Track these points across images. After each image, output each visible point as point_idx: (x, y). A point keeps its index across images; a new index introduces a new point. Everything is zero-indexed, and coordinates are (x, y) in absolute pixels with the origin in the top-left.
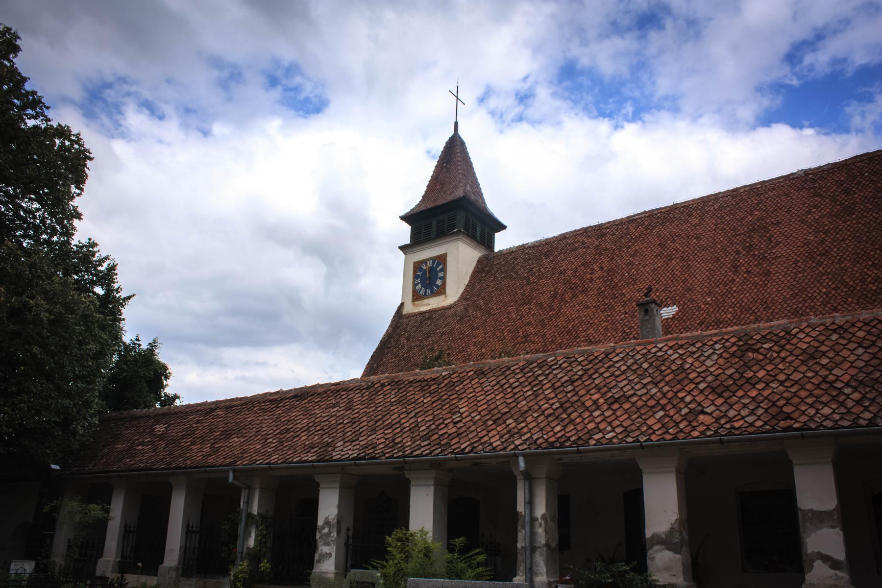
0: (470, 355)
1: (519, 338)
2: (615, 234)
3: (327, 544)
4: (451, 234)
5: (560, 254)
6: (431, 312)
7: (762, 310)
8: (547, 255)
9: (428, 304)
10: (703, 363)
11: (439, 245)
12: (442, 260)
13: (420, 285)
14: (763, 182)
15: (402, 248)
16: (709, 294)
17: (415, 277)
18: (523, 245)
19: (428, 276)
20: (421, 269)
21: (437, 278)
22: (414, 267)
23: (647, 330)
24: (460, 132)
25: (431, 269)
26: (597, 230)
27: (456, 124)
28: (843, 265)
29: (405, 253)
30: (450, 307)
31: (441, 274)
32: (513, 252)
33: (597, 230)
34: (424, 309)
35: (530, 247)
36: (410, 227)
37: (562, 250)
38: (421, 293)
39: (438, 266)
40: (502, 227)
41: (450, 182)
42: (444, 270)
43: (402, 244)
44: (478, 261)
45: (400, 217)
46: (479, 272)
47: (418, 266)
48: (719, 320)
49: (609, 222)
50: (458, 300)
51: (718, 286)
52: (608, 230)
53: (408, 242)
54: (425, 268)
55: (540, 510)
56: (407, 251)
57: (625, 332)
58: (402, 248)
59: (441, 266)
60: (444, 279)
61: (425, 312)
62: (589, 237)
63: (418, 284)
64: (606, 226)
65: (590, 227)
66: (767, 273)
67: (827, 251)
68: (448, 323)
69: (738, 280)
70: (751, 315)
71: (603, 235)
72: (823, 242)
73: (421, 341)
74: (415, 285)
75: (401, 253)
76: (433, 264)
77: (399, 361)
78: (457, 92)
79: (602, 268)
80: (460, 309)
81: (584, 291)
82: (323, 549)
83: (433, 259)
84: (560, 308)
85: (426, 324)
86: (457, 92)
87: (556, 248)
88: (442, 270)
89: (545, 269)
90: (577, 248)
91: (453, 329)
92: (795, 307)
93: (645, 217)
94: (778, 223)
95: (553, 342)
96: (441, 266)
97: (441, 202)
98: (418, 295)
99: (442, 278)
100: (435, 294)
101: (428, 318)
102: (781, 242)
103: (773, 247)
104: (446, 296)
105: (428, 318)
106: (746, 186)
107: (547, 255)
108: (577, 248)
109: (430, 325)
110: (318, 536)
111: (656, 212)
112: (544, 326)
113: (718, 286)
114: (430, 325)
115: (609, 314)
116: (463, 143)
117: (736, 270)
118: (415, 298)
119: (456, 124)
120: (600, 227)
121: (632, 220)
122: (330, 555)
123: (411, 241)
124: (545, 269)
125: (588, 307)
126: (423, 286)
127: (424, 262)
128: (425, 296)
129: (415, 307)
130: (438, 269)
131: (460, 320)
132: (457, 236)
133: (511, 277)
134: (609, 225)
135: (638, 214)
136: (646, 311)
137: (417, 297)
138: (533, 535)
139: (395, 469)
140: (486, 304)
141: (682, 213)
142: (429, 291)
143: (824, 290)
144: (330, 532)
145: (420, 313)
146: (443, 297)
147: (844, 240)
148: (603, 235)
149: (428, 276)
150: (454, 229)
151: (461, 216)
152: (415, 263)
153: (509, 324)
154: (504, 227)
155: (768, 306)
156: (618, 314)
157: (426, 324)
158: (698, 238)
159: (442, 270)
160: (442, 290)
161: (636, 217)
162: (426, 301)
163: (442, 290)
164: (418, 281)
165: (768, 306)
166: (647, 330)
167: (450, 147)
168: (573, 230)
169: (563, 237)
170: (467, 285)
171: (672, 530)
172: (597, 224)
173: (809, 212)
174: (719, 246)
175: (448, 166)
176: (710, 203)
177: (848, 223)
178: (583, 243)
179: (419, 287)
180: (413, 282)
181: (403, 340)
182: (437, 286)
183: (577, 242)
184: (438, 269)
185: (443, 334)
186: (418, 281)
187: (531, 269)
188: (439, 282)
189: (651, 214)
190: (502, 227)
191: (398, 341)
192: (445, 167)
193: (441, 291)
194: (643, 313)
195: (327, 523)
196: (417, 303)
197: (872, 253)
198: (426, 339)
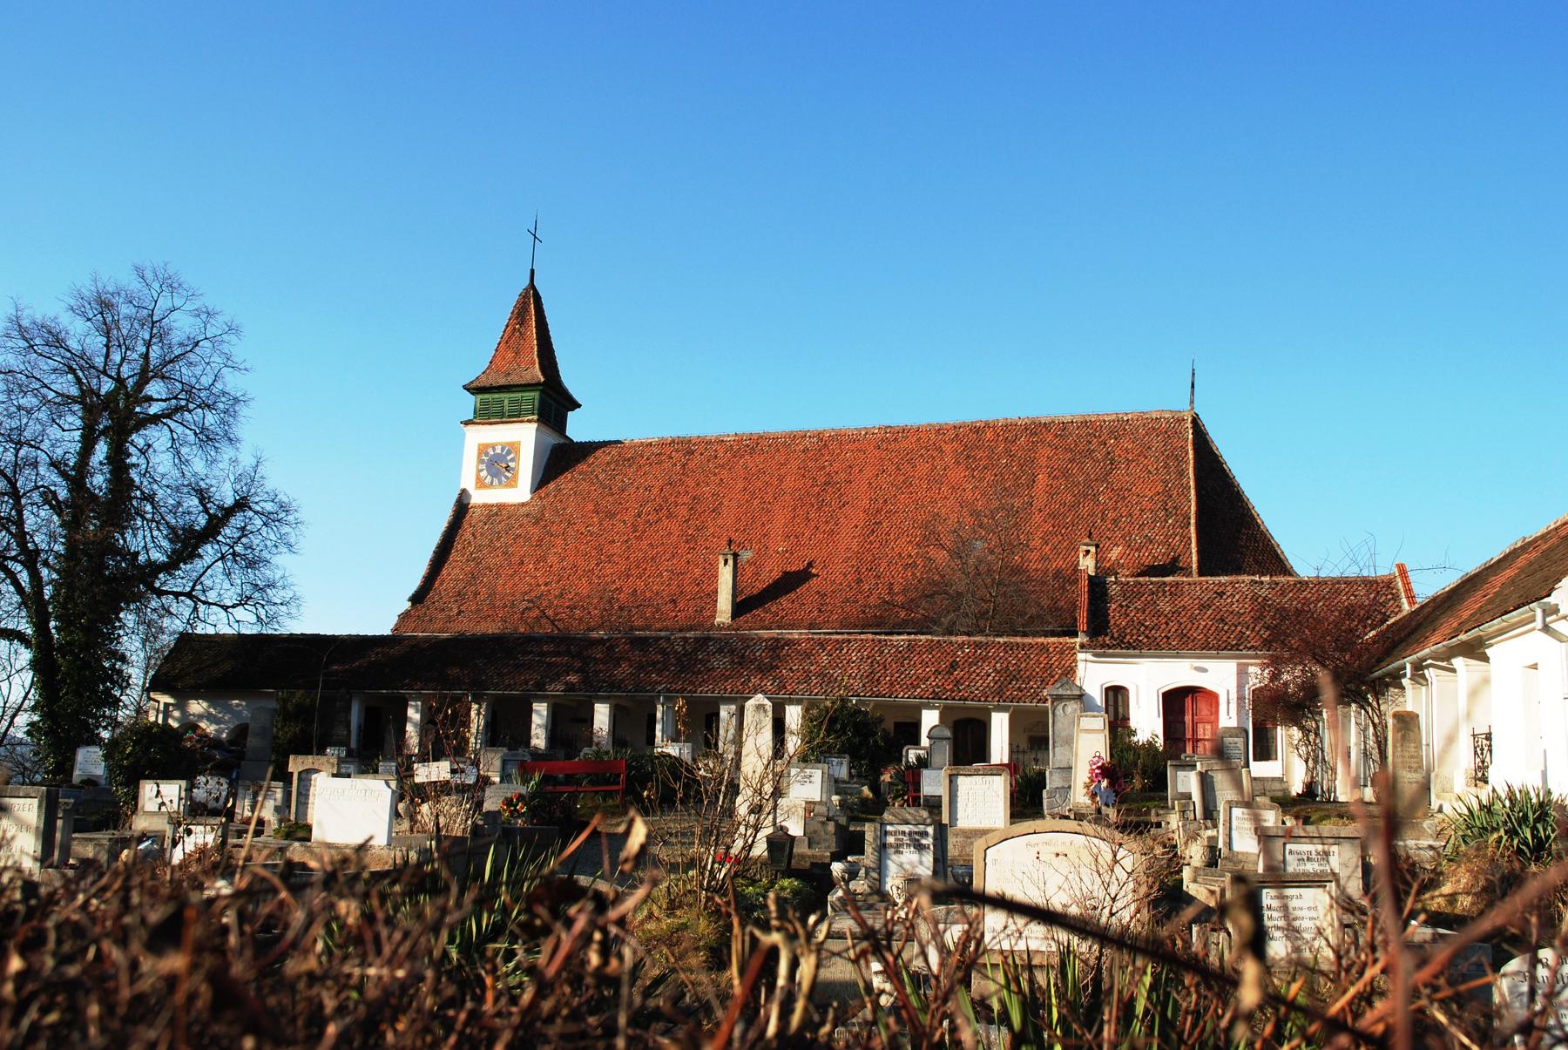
10: (754, 654)
17: (480, 461)
27: (532, 271)
37: (648, 459)
39: (509, 453)
40: (577, 405)
44: (552, 451)
63: (482, 470)
74: (480, 471)
76: (503, 449)
77: (468, 561)
89: (630, 479)
96: (512, 456)
101: (496, 514)
119: (532, 271)
124: (630, 479)
131: (534, 524)
142: (496, 481)
154: (579, 406)
175: (523, 331)
179: (484, 474)
180: (477, 467)
186: (484, 466)
190: (577, 405)
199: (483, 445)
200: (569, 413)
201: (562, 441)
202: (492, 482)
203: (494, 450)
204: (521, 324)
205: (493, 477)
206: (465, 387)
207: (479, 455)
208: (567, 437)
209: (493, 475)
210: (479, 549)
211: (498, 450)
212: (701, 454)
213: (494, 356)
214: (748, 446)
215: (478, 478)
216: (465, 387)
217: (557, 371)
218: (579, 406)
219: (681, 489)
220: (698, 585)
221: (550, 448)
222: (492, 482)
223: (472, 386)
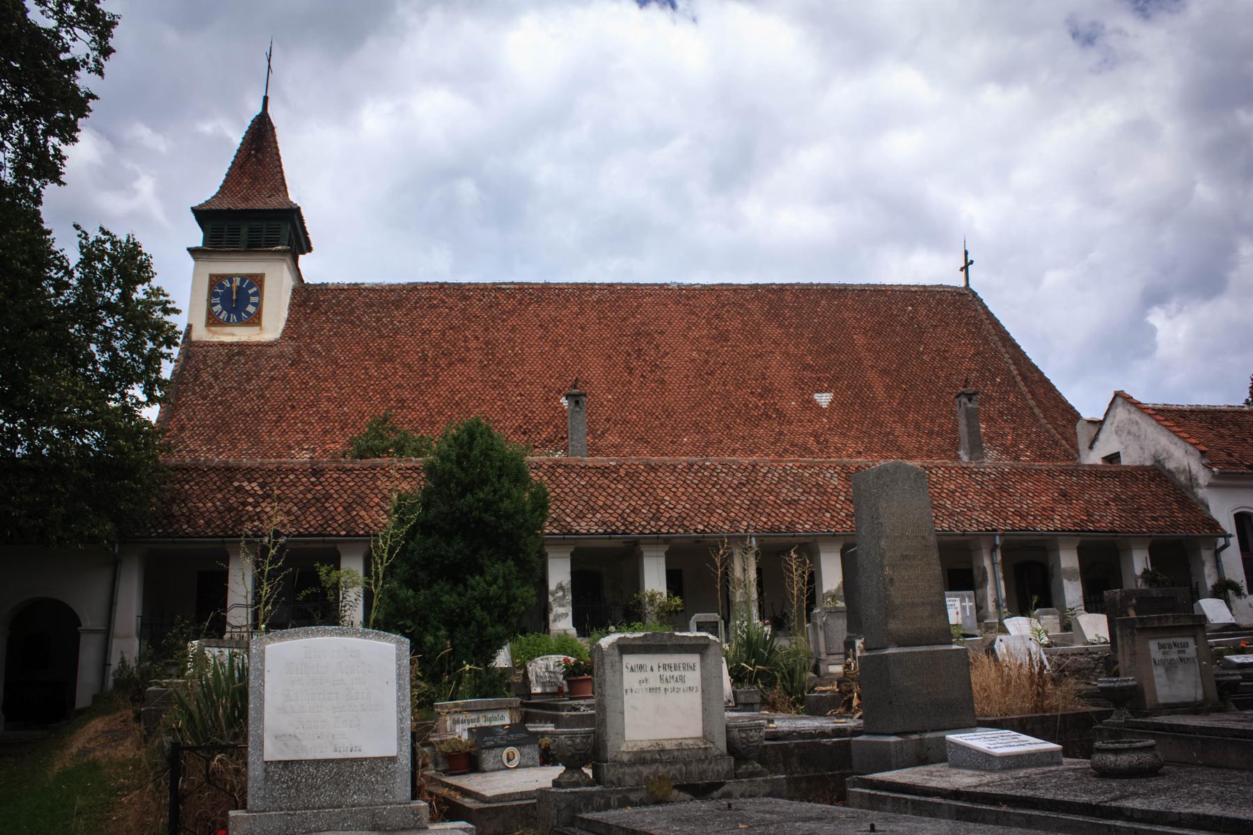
0: (327, 412)
1: (392, 402)
2: (482, 300)
3: (563, 606)
4: (279, 251)
5: (415, 308)
7: (665, 417)
8: (398, 304)
9: (233, 335)
11: (254, 261)
12: (257, 281)
14: (638, 285)
15: (193, 251)
16: (609, 391)
17: (212, 294)
18: (356, 284)
19: (234, 297)
20: (222, 286)
21: (248, 302)
23: (578, 421)
24: (269, 111)
25: (239, 288)
27: (266, 99)
28: (727, 388)
29: (195, 259)
30: (270, 345)
31: (254, 299)
34: (227, 339)
38: (221, 317)
39: (250, 286)
41: (265, 180)
42: (259, 294)
43: (193, 245)
46: (300, 306)
47: (216, 281)
48: (625, 420)
50: (281, 338)
51: (616, 385)
52: (471, 293)
53: (199, 243)
54: (229, 285)
55: (753, 574)
57: (527, 415)
58: (193, 251)
59: (254, 289)
60: (259, 306)
61: (231, 344)
62: (448, 296)
63: (216, 304)
64: (467, 287)
66: (663, 382)
67: (712, 371)
68: (275, 366)
69: (635, 383)
70: (655, 420)
72: (707, 362)
73: (240, 383)
74: (211, 305)
77: (212, 404)
79: (477, 338)
80: (288, 349)
81: (462, 360)
82: (557, 610)
83: (243, 278)
84: (437, 376)
85: (238, 361)
88: (255, 294)
89: (400, 322)
90: (435, 306)
91: (286, 375)
92: (694, 419)
93: (515, 289)
94: (662, 333)
95: (440, 413)
96: (254, 289)
98: (215, 319)
99: (254, 304)
100: (241, 322)
101: (239, 354)
102: (668, 353)
103: (663, 357)
104: (261, 329)
105: (239, 354)
106: (621, 284)
107: (398, 304)
108: (435, 306)
109: (246, 363)
110: (551, 599)
111: (526, 286)
112: (422, 393)
113: (616, 385)
114: (246, 363)
117: (631, 372)
118: (211, 321)
119: (266, 99)
121: (499, 289)
122: (566, 615)
125: (473, 381)
126: (224, 308)
127: (230, 277)
128: (227, 323)
129: (211, 335)
131: (291, 365)
132: (283, 255)
133: (352, 323)
136: (577, 403)
137: (213, 320)
138: (747, 594)
139: (624, 542)
140: (329, 350)
141: (558, 295)
143: (716, 408)
144: (564, 596)
145: (222, 344)
146: (257, 328)
147: (724, 364)
148: (466, 298)
149: (234, 297)
150: (278, 245)
151: (286, 229)
152: (211, 276)
155: (669, 414)
157: (238, 361)
158: (582, 328)
159: (255, 294)
160: (256, 321)
161: (503, 286)
162: (228, 329)
163: (256, 321)
164: (218, 300)
165: (669, 414)
166: (578, 421)
167: (259, 129)
168: (425, 281)
170: (288, 320)
171: (838, 589)
173: (689, 328)
174: (608, 343)
176: (587, 293)
177: (725, 349)
178: (444, 302)
179: (218, 308)
180: (209, 300)
181: (205, 376)
182: (248, 313)
185: (272, 379)
186: (218, 300)
187: (378, 320)
188: (251, 309)
189: (521, 287)
191: (196, 378)
192: (255, 156)
193: (255, 320)
194: (573, 404)
195: (560, 587)
196: (213, 329)
197: (750, 382)
198: (249, 380)
199: (217, 276)
202: (229, 318)
204: (257, 151)
209: (230, 311)
210: (224, 391)
214: (531, 294)
220: (524, 433)
222: (229, 318)
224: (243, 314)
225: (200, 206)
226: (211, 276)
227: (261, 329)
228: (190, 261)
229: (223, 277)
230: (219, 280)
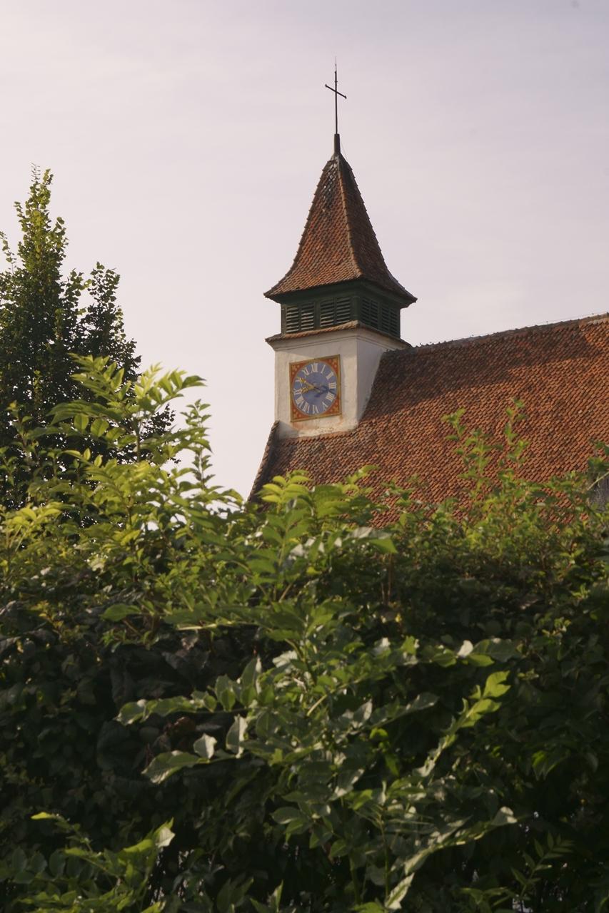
4: (346, 329)
6: (322, 440)
9: (317, 428)
12: (333, 362)
13: (301, 398)
15: (272, 341)
22: (291, 371)
26: (546, 334)
27: (337, 137)
29: (274, 349)
30: (349, 435)
32: (430, 353)
33: (546, 334)
35: (453, 348)
36: (279, 305)
37: (499, 360)
38: (304, 410)
39: (327, 372)
40: (409, 299)
42: (338, 378)
44: (381, 361)
45: (265, 294)
47: (296, 370)
49: (562, 324)
56: (277, 346)
58: (272, 341)
62: (534, 345)
63: (299, 396)
65: (536, 327)
71: (553, 344)
74: (293, 398)
75: (270, 348)
76: (320, 368)
78: (336, 82)
80: (364, 437)
86: (336, 82)
87: (492, 355)
88: (332, 380)
96: (332, 374)
97: (327, 279)
98: (299, 413)
101: (319, 450)
115: (558, 467)
116: (345, 170)
119: (337, 137)
120: (549, 329)
123: (282, 330)
126: (306, 400)
128: (309, 416)
130: (328, 377)
131: (365, 457)
134: (561, 328)
135: (599, 317)
137: (297, 414)
146: (338, 418)
152: (292, 365)
153: (434, 469)
154: (414, 300)
156: (568, 468)
159: (332, 380)
160: (336, 409)
161: (595, 322)
162: (315, 422)
163: (336, 409)
169: (500, 338)
172: (546, 324)
178: (528, 354)
179: (300, 400)
180: (291, 393)
182: (327, 402)
183: (520, 350)
184: (328, 377)
190: (409, 299)
196: (300, 423)
200: (403, 312)
201: (393, 347)
203: (310, 370)
204: (327, 207)
205: (311, 404)
206: (268, 295)
207: (293, 377)
208: (403, 342)
211: (315, 370)
212: (566, 345)
213: (300, 252)
215: (293, 406)
216: (268, 295)
217: (381, 259)
218: (414, 300)
219: (543, 395)
221: (379, 359)
223: (275, 292)
224: (323, 403)
225: (275, 288)
226: (292, 365)
227: (341, 418)
228: (269, 348)
229: (302, 365)
230: (298, 369)
